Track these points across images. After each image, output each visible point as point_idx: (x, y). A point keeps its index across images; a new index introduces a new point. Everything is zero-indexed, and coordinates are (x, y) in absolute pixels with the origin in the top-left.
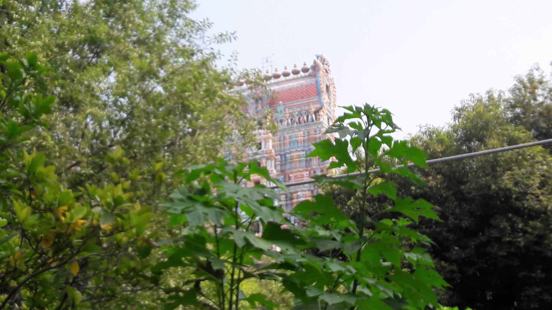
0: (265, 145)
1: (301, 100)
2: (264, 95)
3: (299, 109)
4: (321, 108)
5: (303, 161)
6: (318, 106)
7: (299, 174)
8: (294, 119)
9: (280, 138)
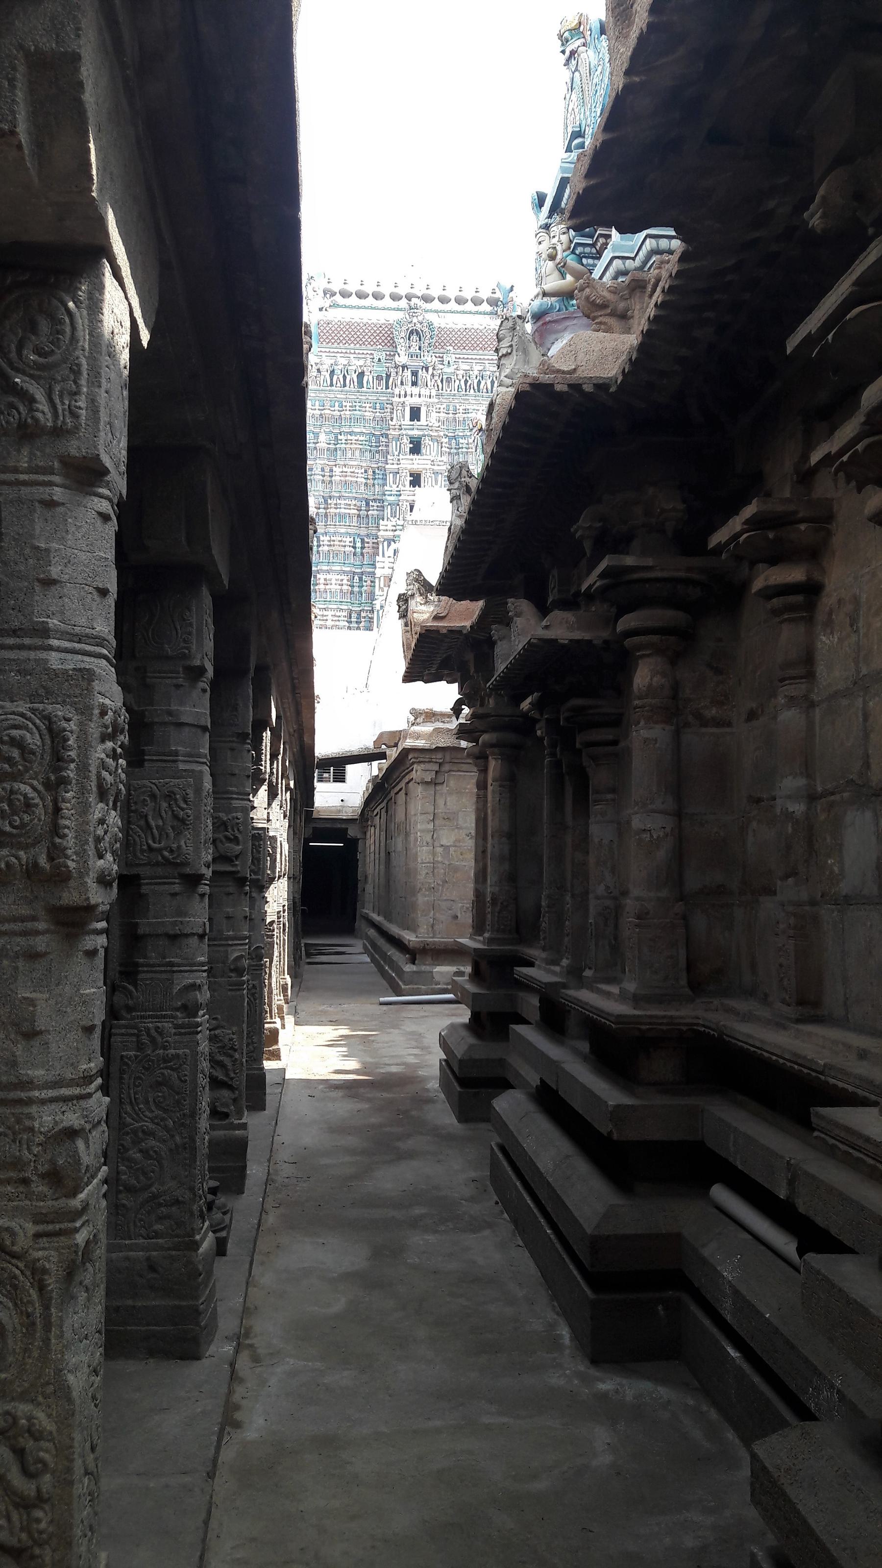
1: (481, 352)
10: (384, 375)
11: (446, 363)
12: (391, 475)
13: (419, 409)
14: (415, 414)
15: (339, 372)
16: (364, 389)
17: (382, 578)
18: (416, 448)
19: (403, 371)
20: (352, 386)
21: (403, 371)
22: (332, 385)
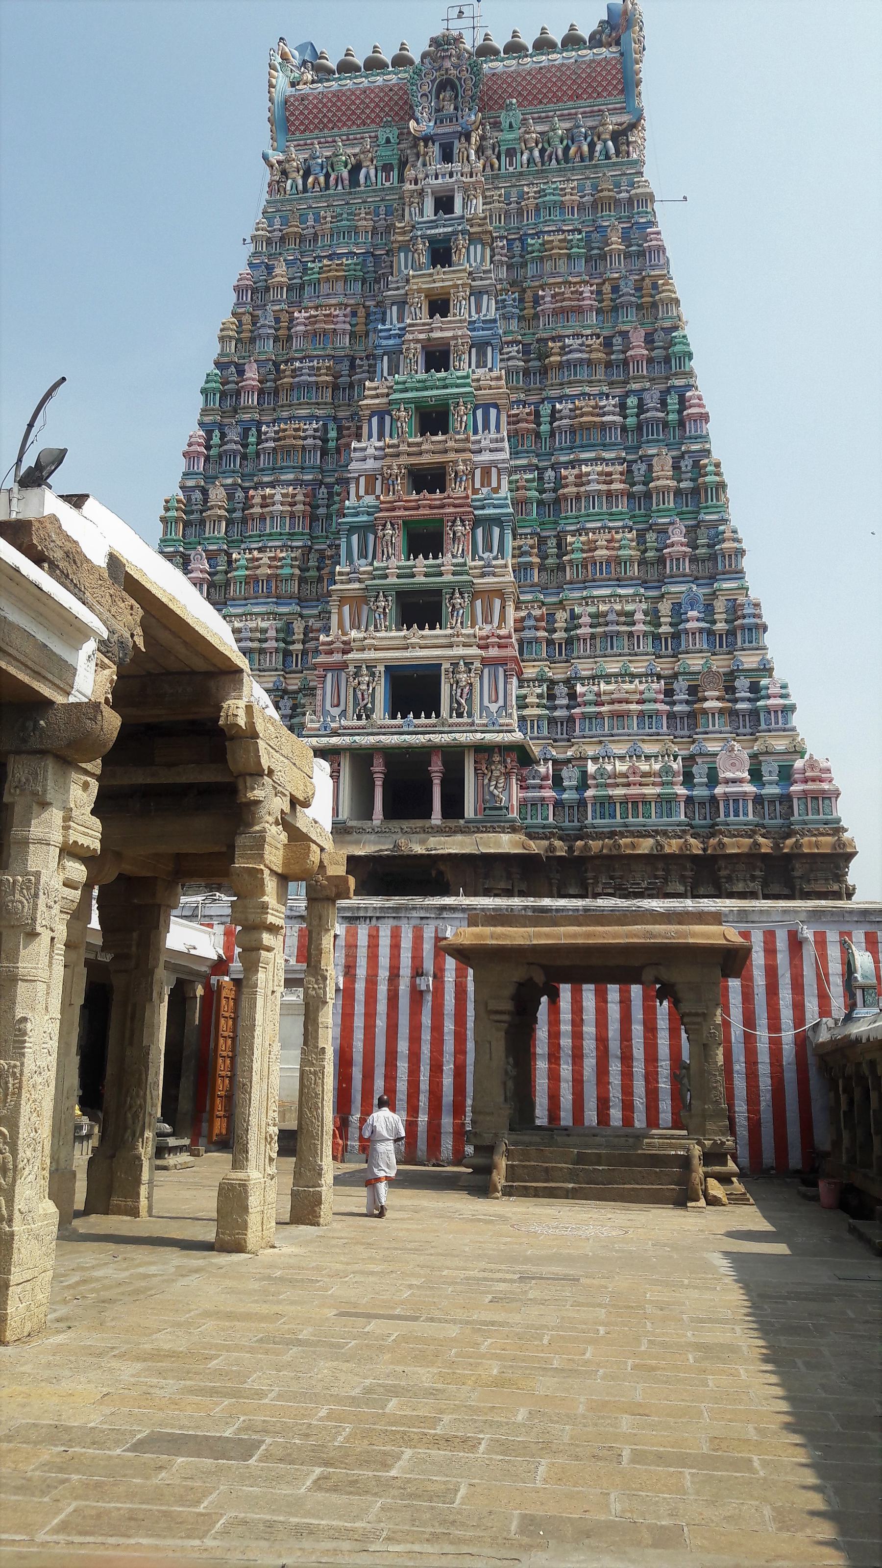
2: (465, 75)
3: (567, 125)
4: (633, 126)
5: (579, 256)
6: (625, 118)
7: (567, 292)
8: (549, 150)
9: (508, 195)
11: (505, 125)
12: (395, 308)
13: (451, 199)
14: (444, 204)
15: (318, 169)
16: (362, 188)
17: (362, 480)
18: (441, 254)
19: (426, 146)
20: (340, 187)
21: (426, 146)
22: (305, 190)
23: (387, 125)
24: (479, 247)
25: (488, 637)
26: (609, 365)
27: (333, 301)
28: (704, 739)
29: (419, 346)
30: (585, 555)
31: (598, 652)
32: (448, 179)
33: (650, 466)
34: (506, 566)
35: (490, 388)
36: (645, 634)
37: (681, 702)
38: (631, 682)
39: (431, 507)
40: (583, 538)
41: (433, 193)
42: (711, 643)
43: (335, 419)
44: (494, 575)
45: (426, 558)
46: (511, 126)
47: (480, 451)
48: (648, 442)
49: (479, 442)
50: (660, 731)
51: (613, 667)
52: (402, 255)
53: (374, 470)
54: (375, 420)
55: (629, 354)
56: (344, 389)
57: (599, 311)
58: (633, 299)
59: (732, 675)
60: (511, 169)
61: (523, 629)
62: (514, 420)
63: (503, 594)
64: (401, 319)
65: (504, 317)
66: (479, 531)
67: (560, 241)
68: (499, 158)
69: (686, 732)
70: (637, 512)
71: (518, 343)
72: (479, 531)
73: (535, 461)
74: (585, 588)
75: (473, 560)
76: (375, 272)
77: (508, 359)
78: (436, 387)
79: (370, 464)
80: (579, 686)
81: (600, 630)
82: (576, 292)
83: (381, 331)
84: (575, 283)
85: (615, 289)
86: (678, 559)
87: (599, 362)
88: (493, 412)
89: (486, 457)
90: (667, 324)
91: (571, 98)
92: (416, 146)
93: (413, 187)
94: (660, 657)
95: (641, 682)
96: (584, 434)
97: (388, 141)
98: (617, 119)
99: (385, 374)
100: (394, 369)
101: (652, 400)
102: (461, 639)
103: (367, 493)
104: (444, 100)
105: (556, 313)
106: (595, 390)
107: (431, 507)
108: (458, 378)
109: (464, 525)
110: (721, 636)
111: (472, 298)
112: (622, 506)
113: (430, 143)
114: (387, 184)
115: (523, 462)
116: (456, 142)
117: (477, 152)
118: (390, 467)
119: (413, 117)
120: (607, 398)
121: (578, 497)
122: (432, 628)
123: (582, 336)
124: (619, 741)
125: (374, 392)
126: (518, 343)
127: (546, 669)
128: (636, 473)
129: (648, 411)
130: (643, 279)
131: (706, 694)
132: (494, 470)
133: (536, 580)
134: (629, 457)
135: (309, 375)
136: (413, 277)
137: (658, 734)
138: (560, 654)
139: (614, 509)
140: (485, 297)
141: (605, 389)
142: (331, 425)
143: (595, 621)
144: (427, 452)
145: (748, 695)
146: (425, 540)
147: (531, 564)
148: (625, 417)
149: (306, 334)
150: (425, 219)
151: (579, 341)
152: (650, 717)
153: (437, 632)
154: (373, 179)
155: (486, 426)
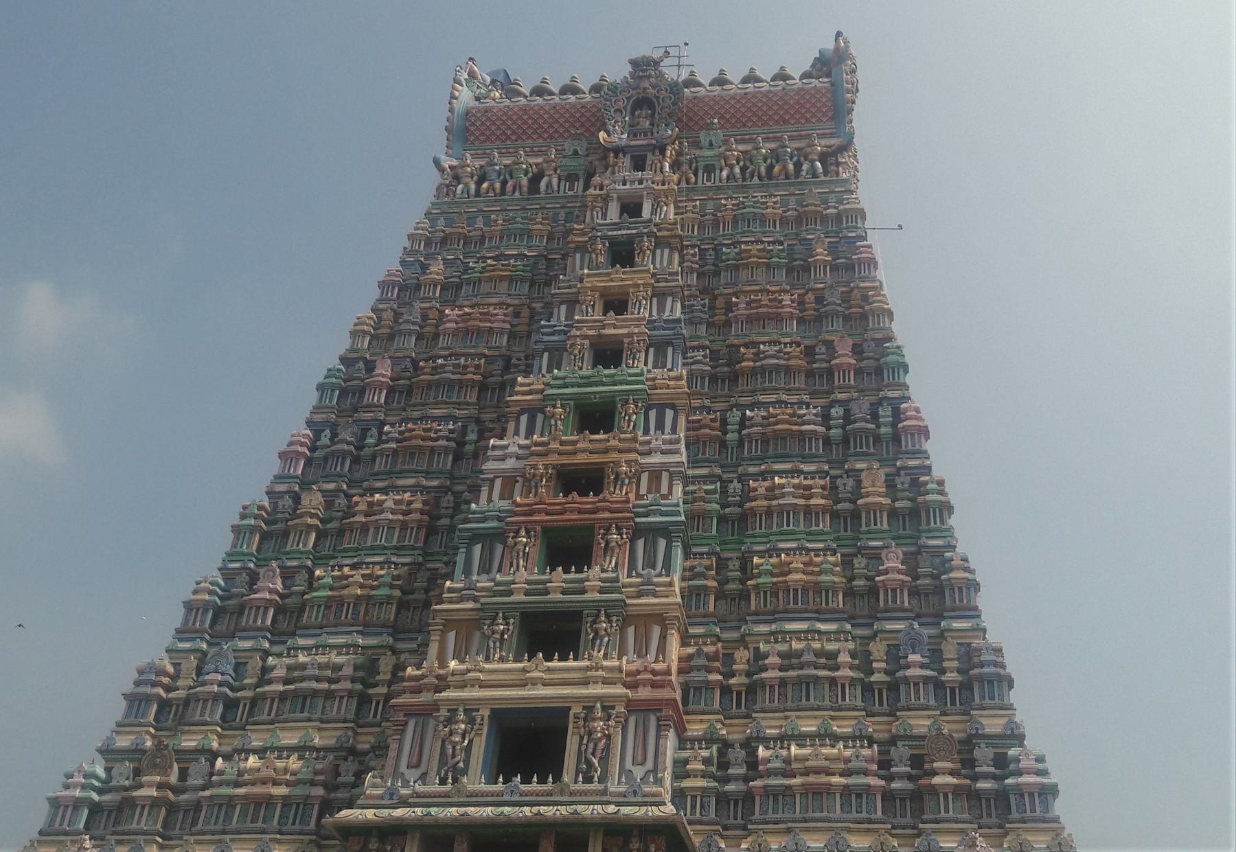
0: (654, 211)
3: (773, 145)
5: (779, 266)
6: (834, 141)
8: (751, 168)
9: (703, 208)
10: (581, 173)
12: (563, 308)
14: (631, 208)
18: (623, 254)
20: (517, 194)
21: (616, 156)
23: (576, 137)
24: (666, 251)
25: (638, 672)
26: (810, 374)
27: (494, 300)
28: (935, 831)
29: (587, 342)
30: (775, 580)
31: (789, 704)
32: (637, 185)
33: (859, 483)
34: (671, 584)
35: (668, 387)
36: (853, 682)
37: (901, 776)
38: (833, 746)
39: (580, 512)
40: (774, 560)
41: (619, 198)
42: (940, 699)
43: (478, 421)
44: (655, 595)
45: (566, 571)
46: (711, 144)
47: (649, 453)
48: (856, 455)
49: (649, 442)
50: (873, 816)
51: (809, 727)
52: (578, 256)
53: (515, 470)
54: (524, 419)
55: (834, 362)
56: (493, 390)
57: (801, 321)
58: (839, 309)
59: (969, 743)
60: (709, 184)
61: (690, 670)
62: (693, 426)
63: (665, 619)
64: (570, 316)
65: (690, 322)
66: (640, 543)
67: (758, 250)
68: (696, 175)
69: (908, 820)
70: (842, 533)
71: (704, 348)
72: (640, 543)
73: (718, 471)
74: (774, 621)
75: (629, 576)
76: (547, 274)
77: (692, 364)
78: (603, 384)
79: (510, 464)
80: (761, 749)
81: (792, 673)
82: (775, 299)
83: (544, 327)
84: (773, 292)
85: (819, 300)
86: (894, 590)
87: (799, 369)
88: (669, 414)
89: (656, 459)
90: (879, 335)
91: (777, 122)
92: (605, 157)
93: (598, 192)
94: (873, 716)
95: (845, 747)
96: (778, 444)
97: (576, 153)
98: (824, 142)
99: (544, 371)
100: (555, 364)
101: (861, 409)
102: (600, 673)
103: (502, 497)
104: (639, 117)
105: (750, 319)
106: (794, 399)
107: (580, 512)
108: (630, 375)
109: (621, 534)
110: (953, 690)
111: (655, 300)
112: (824, 525)
113: (621, 155)
114: (571, 193)
115: (704, 471)
116: (650, 156)
117: (671, 166)
118: (534, 467)
119: (603, 127)
120: (808, 408)
121: (769, 512)
122: (563, 658)
123: (780, 343)
124: (816, 830)
125: (525, 388)
126: (704, 348)
127: (719, 726)
128: (841, 488)
129: (855, 422)
130: (852, 290)
131: (935, 765)
132: (665, 475)
133: (712, 608)
134: (832, 472)
135: (453, 373)
136: (588, 275)
137: (870, 821)
138: (739, 706)
139: (814, 528)
140: (669, 299)
141: (805, 398)
142: (472, 426)
143: (786, 662)
144: (584, 450)
145: (992, 769)
146: (569, 549)
147: (706, 588)
148: (829, 428)
149: (455, 333)
150: (608, 221)
151: (777, 348)
152: (859, 796)
153: (571, 664)
154: (555, 187)
155: (660, 426)
